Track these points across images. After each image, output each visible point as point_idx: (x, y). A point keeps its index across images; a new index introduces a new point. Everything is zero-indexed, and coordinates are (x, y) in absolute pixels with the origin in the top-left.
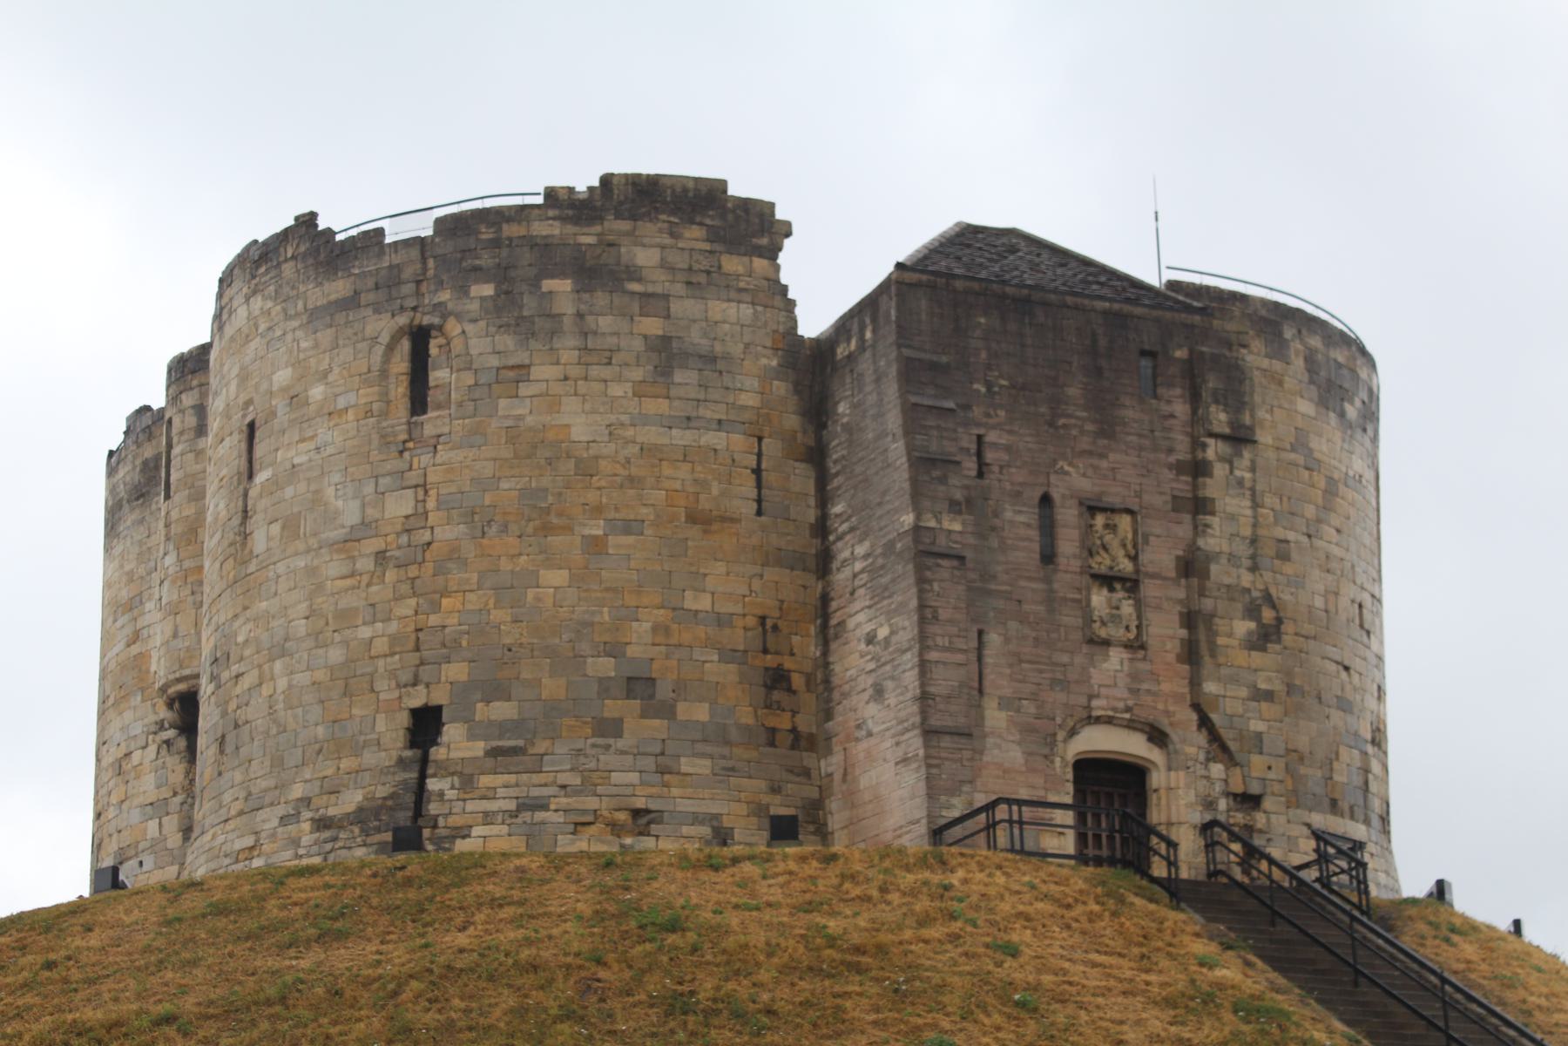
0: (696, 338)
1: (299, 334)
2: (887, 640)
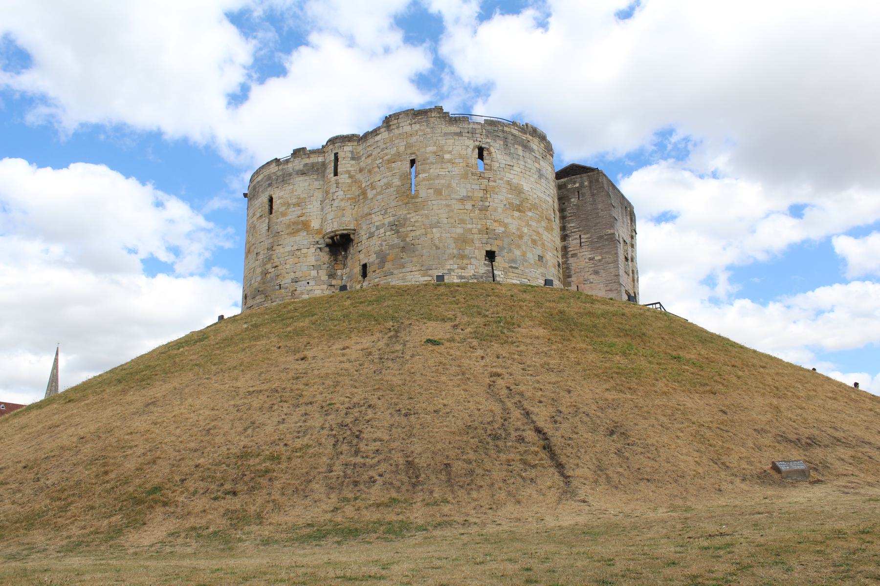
0: (544, 172)
1: (440, 138)
2: (600, 261)
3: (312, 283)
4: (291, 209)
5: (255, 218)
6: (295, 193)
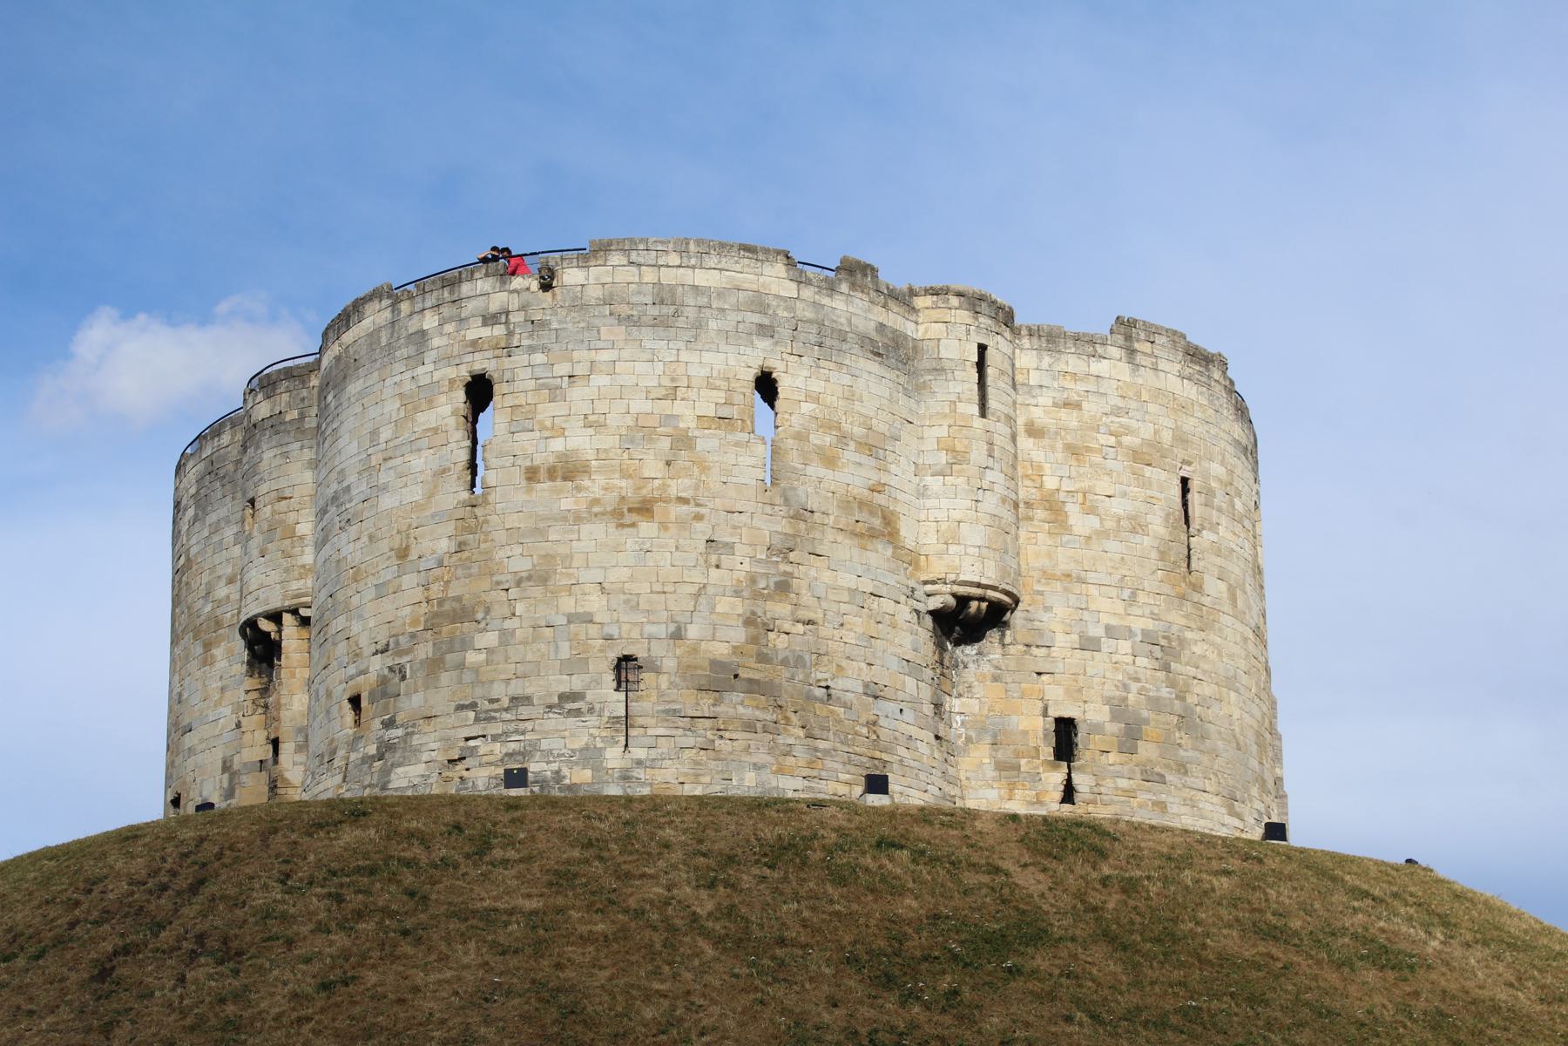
3: (909, 715)
4: (850, 454)
5: (678, 408)
6: (857, 406)
